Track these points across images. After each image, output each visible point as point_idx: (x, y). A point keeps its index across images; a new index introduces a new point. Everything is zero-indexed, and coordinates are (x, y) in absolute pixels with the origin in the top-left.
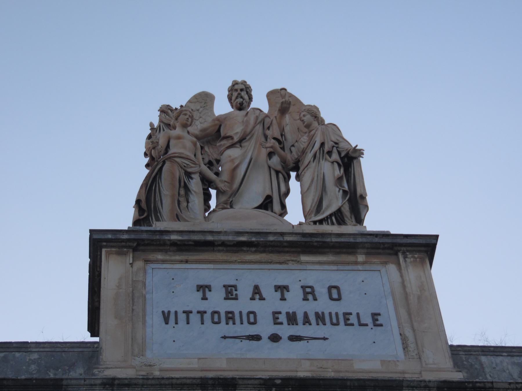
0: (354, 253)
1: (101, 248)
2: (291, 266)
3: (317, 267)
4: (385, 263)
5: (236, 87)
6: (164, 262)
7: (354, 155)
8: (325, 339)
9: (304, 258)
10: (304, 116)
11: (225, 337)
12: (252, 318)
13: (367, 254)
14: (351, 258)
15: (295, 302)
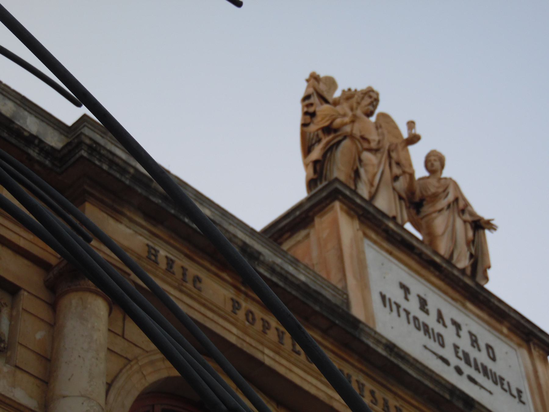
0: (501, 322)
1: (336, 199)
2: (458, 305)
3: (476, 319)
4: (520, 345)
5: (372, 94)
6: (375, 242)
7: (483, 225)
8: (491, 393)
9: (469, 305)
10: (435, 160)
11: (425, 347)
12: (440, 340)
13: (509, 329)
14: (498, 325)
15: (465, 344)
